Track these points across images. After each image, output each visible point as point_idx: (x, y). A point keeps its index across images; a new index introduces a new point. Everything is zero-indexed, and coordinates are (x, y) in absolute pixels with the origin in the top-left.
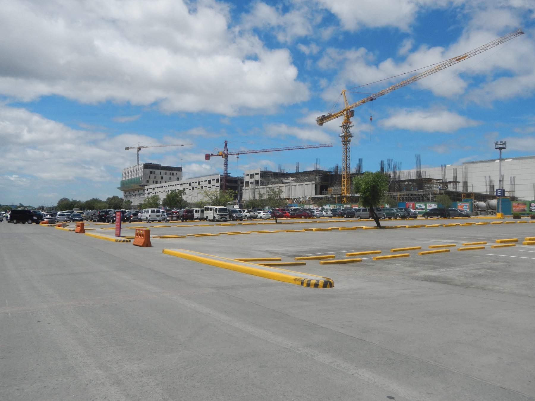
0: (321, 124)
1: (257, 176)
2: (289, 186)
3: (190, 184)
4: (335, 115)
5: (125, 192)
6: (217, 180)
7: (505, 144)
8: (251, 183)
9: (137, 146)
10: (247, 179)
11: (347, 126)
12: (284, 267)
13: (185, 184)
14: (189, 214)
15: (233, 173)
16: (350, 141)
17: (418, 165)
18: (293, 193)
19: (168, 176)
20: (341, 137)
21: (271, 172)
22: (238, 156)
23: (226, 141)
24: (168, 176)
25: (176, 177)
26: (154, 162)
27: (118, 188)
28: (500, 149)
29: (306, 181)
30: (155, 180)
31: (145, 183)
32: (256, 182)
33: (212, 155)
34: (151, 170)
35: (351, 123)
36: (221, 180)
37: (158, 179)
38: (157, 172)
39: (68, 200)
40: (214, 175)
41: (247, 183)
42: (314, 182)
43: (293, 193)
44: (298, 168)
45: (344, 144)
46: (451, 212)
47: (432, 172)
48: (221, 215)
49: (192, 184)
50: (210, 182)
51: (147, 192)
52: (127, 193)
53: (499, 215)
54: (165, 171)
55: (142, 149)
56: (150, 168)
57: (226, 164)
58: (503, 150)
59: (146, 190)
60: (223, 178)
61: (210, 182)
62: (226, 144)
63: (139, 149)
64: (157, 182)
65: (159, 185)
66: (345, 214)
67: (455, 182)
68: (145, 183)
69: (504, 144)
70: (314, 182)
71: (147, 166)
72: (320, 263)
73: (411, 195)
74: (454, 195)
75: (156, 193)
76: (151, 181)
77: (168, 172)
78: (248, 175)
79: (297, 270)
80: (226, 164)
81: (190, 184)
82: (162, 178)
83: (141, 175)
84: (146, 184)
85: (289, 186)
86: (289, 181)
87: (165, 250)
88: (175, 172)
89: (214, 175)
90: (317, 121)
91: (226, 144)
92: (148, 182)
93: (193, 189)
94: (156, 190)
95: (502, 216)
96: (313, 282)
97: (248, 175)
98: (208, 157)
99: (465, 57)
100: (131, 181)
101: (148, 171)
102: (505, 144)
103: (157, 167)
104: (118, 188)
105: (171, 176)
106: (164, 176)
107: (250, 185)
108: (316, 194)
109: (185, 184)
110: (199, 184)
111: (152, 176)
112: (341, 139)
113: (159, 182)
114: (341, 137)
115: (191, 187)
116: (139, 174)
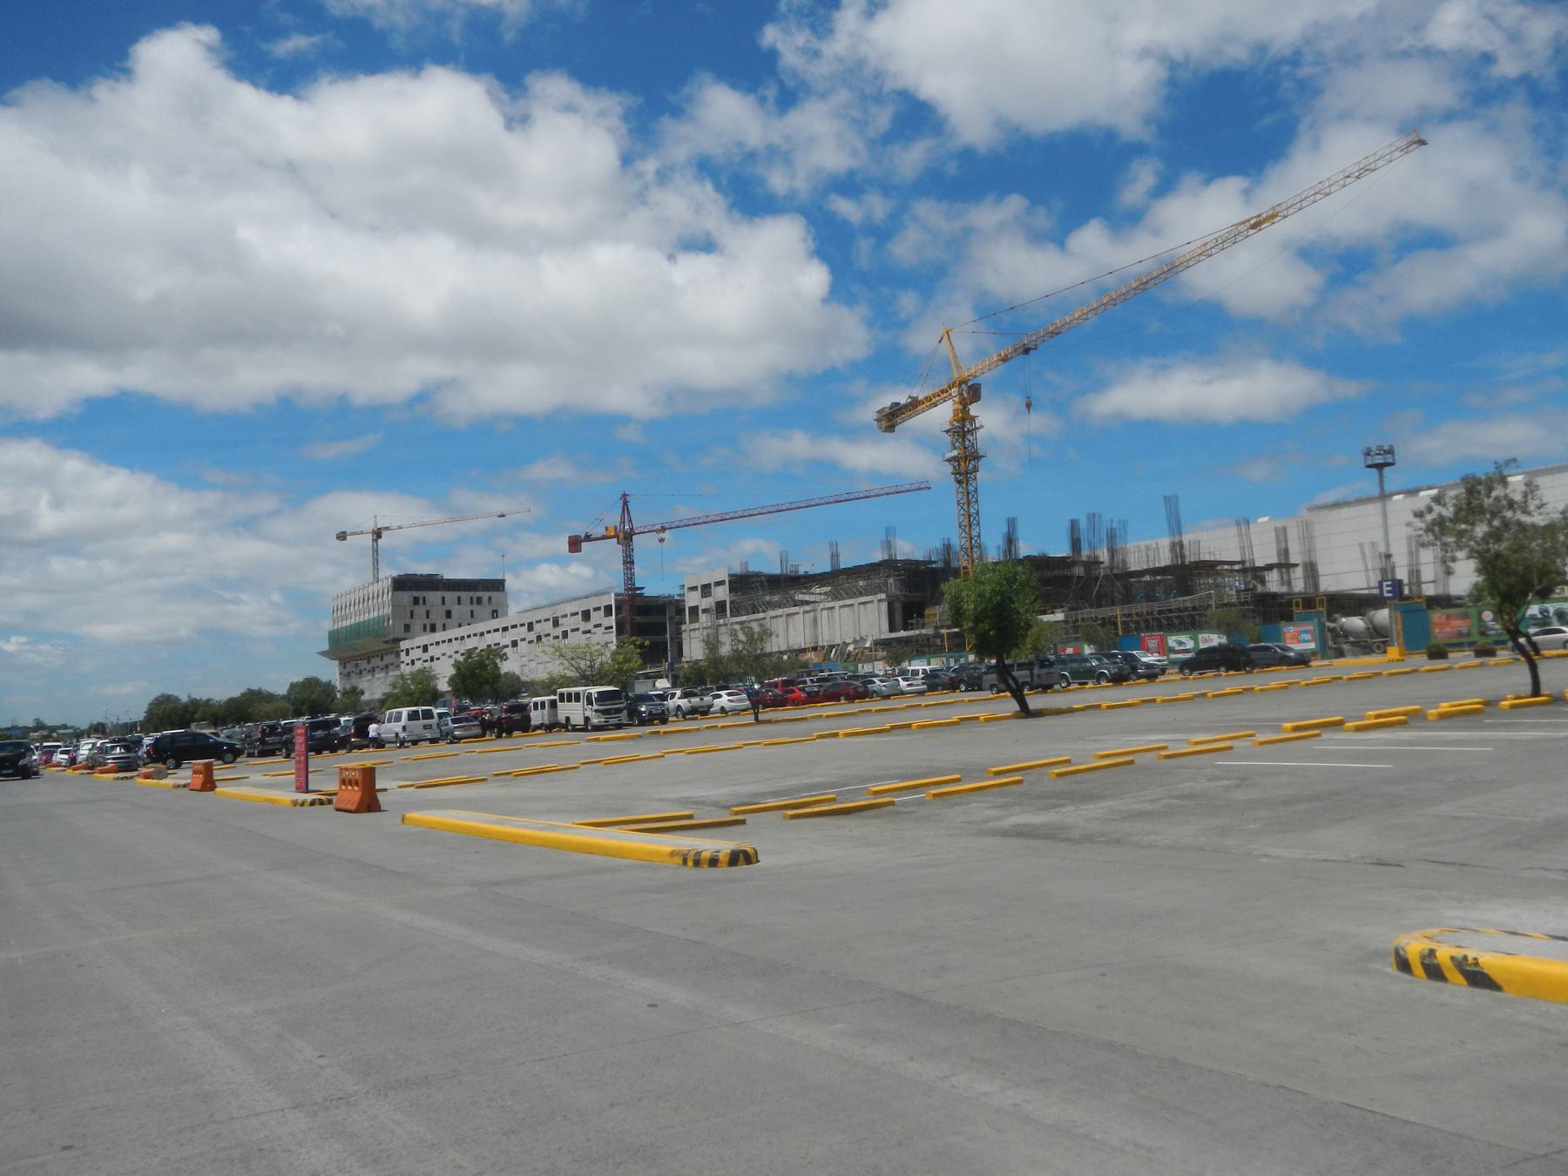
0: (890, 428)
1: (720, 589)
2: (814, 610)
3: (530, 627)
4: (928, 399)
5: (343, 664)
6: (608, 610)
7: (1390, 452)
8: (704, 611)
9: (370, 526)
10: (692, 599)
11: (963, 428)
12: (703, 831)
13: (514, 626)
14: (517, 716)
15: (653, 586)
16: (975, 470)
17: (1176, 526)
18: (826, 629)
19: (466, 609)
20: (949, 460)
21: (758, 575)
22: (662, 535)
23: (624, 495)
24: (466, 609)
25: (489, 609)
26: (423, 569)
27: (323, 654)
28: (1380, 467)
29: (861, 594)
30: (428, 622)
32: (720, 607)
33: (588, 538)
34: (416, 594)
35: (973, 419)
36: (619, 609)
37: (439, 620)
38: (433, 597)
39: (177, 699)
40: (597, 594)
41: (694, 610)
42: (883, 596)
43: (826, 629)
44: (835, 556)
45: (959, 482)
46: (1255, 655)
47: (1215, 542)
48: (605, 712)
49: (537, 627)
50: (586, 616)
51: (408, 659)
52: (350, 667)
53: (1393, 652)
54: (456, 594)
55: (384, 534)
57: (629, 562)
58: (1386, 470)
59: (403, 654)
60: (623, 601)
61: (586, 616)
62: (625, 503)
63: (378, 534)
64: (433, 629)
65: (438, 636)
66: (962, 681)
67: (1285, 566)
69: (1387, 452)
70: (883, 596)
71: (401, 584)
72: (785, 817)
73: (1160, 612)
74: (1281, 604)
75: (432, 659)
76: (417, 625)
77: (465, 595)
78: (694, 589)
79: (712, 837)
80: (629, 562)
81: (530, 627)
82: (449, 614)
83: (388, 610)
85: (814, 610)
86: (812, 598)
87: (408, 815)
88: (485, 595)
89: (597, 594)
90: (878, 420)
91: (625, 503)
92: (407, 628)
93: (539, 638)
94: (433, 651)
95: (1401, 654)
96: (706, 855)
97: (694, 589)
98: (575, 544)
99: (1273, 216)
100: (357, 631)
101: (406, 597)
102: (1390, 452)
103: (432, 583)
104: (323, 654)
105: (475, 607)
106: (455, 610)
107: (703, 617)
108: (892, 629)
109: (514, 626)
110: (556, 623)
111: (420, 610)
112: (949, 468)
113: (439, 626)
114: (949, 460)
115: (532, 636)
116: (382, 608)
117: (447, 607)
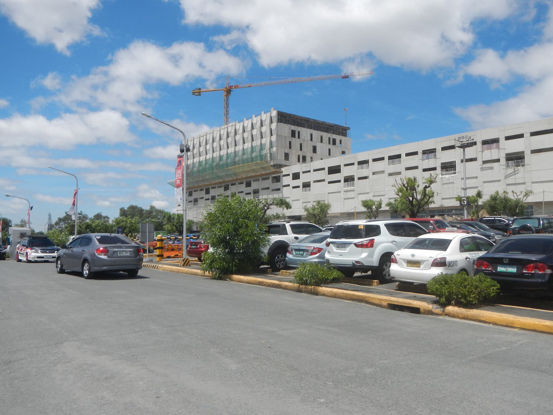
30: (301, 154)
31: (280, 159)
34: (294, 128)
38: (305, 132)
52: (195, 195)
56: (286, 122)
59: (286, 180)
63: (229, 91)
68: (280, 159)
76: (293, 157)
77: (326, 135)
82: (315, 150)
84: (284, 162)
88: (338, 138)
92: (287, 156)
101: (287, 129)
105: (331, 146)
106: (319, 146)
111: (296, 142)
113: (308, 159)
117: (313, 143)
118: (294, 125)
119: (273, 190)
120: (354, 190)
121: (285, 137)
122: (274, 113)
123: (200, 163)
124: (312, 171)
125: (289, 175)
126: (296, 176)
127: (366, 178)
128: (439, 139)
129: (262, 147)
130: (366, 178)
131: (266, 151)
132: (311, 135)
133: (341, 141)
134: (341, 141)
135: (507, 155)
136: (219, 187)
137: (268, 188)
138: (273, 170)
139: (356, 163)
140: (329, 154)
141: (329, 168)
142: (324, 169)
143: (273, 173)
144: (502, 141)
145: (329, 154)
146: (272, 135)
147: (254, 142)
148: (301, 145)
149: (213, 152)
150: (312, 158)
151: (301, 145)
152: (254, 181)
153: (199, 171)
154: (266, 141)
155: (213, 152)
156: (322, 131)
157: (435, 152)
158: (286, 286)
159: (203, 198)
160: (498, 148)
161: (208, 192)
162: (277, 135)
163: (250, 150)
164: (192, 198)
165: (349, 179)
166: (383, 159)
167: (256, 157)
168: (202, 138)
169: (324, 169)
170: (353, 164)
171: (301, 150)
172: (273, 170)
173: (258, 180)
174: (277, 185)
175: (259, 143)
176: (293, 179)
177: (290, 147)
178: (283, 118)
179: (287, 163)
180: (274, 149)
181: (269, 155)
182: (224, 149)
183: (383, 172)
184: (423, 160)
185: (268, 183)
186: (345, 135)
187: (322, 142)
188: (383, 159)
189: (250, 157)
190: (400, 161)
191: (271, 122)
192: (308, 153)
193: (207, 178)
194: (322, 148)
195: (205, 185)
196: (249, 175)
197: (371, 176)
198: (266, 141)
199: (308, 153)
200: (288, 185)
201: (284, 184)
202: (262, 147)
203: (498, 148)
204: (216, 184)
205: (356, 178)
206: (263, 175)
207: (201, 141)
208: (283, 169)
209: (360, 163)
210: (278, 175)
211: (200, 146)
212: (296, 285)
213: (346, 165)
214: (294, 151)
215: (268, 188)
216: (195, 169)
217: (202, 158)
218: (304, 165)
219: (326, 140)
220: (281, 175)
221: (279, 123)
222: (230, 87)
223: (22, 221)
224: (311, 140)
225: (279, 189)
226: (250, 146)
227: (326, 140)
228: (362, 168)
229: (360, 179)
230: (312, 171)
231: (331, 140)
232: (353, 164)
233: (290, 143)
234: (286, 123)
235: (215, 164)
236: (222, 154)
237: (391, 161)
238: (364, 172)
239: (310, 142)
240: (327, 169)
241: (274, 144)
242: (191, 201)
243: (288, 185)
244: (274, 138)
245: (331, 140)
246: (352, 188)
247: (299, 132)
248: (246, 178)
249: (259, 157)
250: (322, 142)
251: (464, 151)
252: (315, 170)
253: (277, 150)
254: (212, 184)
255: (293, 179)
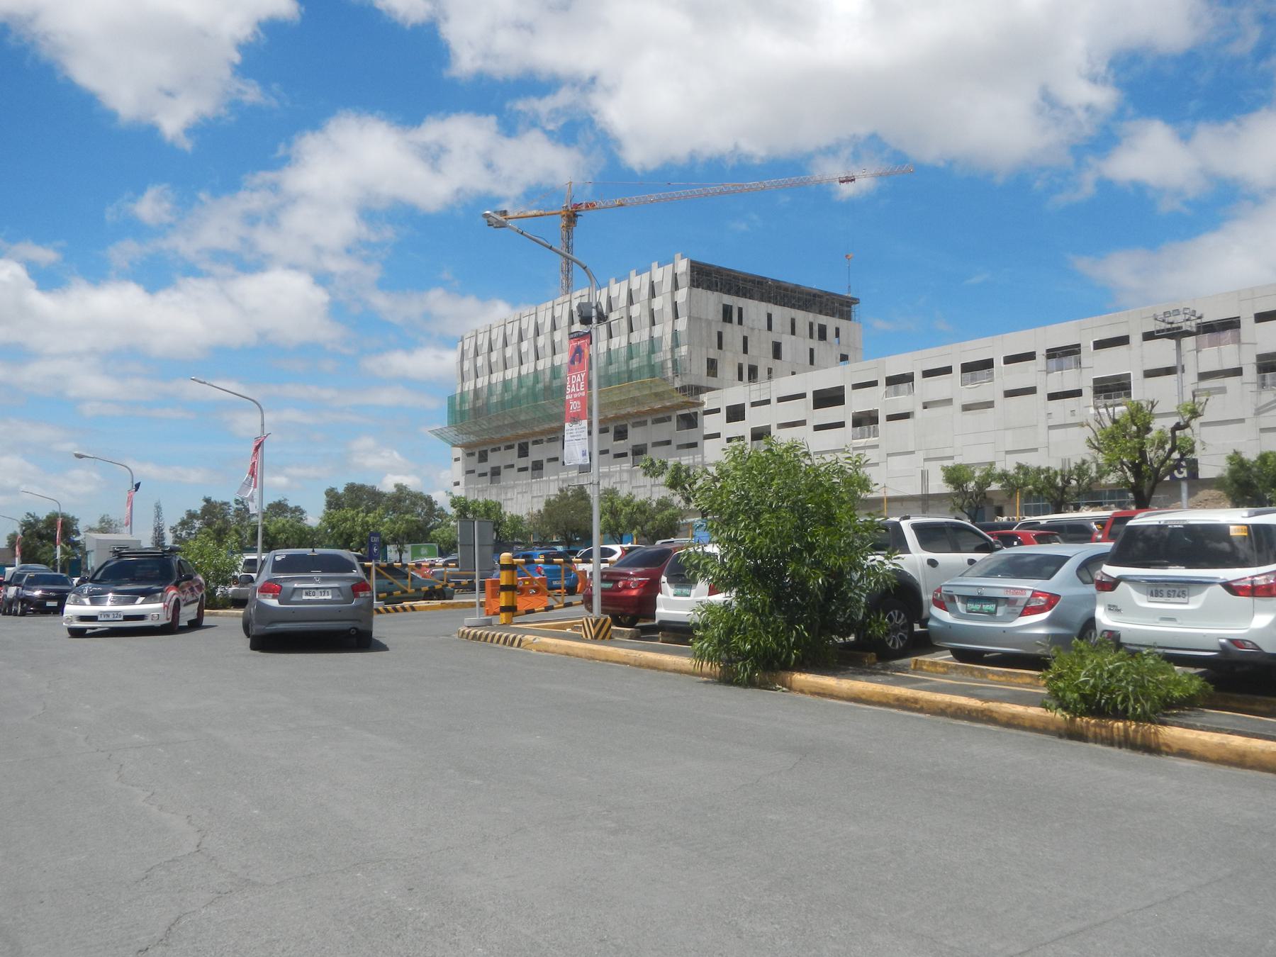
5: (478, 452)
30: (746, 361)
31: (698, 373)
34: (728, 299)
38: (755, 310)
52: (494, 460)
56: (711, 287)
59: (710, 424)
63: (571, 217)
68: (698, 373)
76: (727, 370)
77: (803, 318)
82: (777, 351)
84: (705, 381)
88: (831, 323)
92: (712, 366)
101: (712, 302)
105: (815, 343)
106: (787, 342)
111: (733, 333)
113: (762, 372)
117: (773, 336)
118: (729, 292)
119: (680, 447)
120: (876, 446)
121: (709, 322)
122: (682, 266)
123: (506, 384)
124: (774, 401)
125: (718, 411)
126: (736, 413)
127: (906, 416)
128: (1087, 322)
129: (653, 345)
130: (906, 416)
131: (664, 355)
132: (769, 317)
133: (837, 330)
134: (837, 330)
135: (1260, 357)
136: (550, 440)
137: (668, 443)
138: (680, 398)
139: (882, 382)
140: (812, 362)
141: (816, 393)
142: (803, 396)
143: (681, 406)
144: (1248, 324)
145: (812, 362)
146: (676, 316)
147: (635, 334)
148: (745, 339)
149: (537, 358)
150: (770, 371)
151: (745, 339)
152: (635, 425)
153: (502, 404)
154: (663, 331)
155: (537, 358)
156: (793, 306)
157: (1079, 352)
158: (1014, 716)
159: (512, 466)
160: (1238, 341)
161: (523, 452)
162: (690, 318)
163: (624, 352)
164: (486, 467)
165: (865, 420)
166: (948, 370)
167: (639, 369)
168: (509, 327)
169: (803, 396)
170: (874, 384)
171: (745, 351)
172: (680, 398)
173: (644, 423)
174: (688, 435)
175: (646, 337)
176: (729, 420)
177: (720, 347)
178: (703, 276)
179: (712, 382)
180: (683, 350)
181: (670, 364)
182: (562, 351)
183: (949, 402)
184: (1048, 373)
185: (669, 430)
186: (847, 316)
187: (793, 333)
188: (948, 370)
189: (624, 368)
190: (992, 374)
191: (676, 286)
192: (764, 360)
193: (522, 418)
194: (795, 347)
195: (518, 437)
196: (623, 412)
197: (919, 412)
198: (663, 331)
199: (764, 360)
200: (718, 435)
201: (706, 433)
202: (653, 345)
203: (1238, 341)
204: (543, 433)
205: (882, 418)
206: (657, 411)
207: (508, 332)
208: (704, 397)
209: (892, 381)
210: (693, 410)
211: (505, 344)
212: (1059, 716)
213: (857, 386)
214: (729, 355)
215: (668, 443)
216: (494, 399)
217: (511, 373)
218: (754, 386)
219: (802, 327)
220: (700, 410)
221: (695, 290)
222: (576, 206)
223: (102, 520)
224: (770, 328)
225: (694, 445)
226: (624, 343)
227: (802, 327)
228: (897, 394)
229: (891, 418)
230: (774, 401)
231: (816, 328)
232: (874, 384)
233: (720, 335)
234: (709, 288)
235: (540, 386)
236: (557, 363)
237: (969, 375)
238: (902, 401)
239: (765, 332)
240: (810, 397)
241: (683, 338)
242: (485, 474)
243: (718, 435)
244: (682, 325)
245: (816, 328)
246: (872, 440)
247: (740, 310)
248: (617, 418)
249: (646, 370)
250: (793, 333)
251: (1179, 345)
252: (780, 400)
253: (690, 352)
254: (534, 434)
255: (729, 420)
